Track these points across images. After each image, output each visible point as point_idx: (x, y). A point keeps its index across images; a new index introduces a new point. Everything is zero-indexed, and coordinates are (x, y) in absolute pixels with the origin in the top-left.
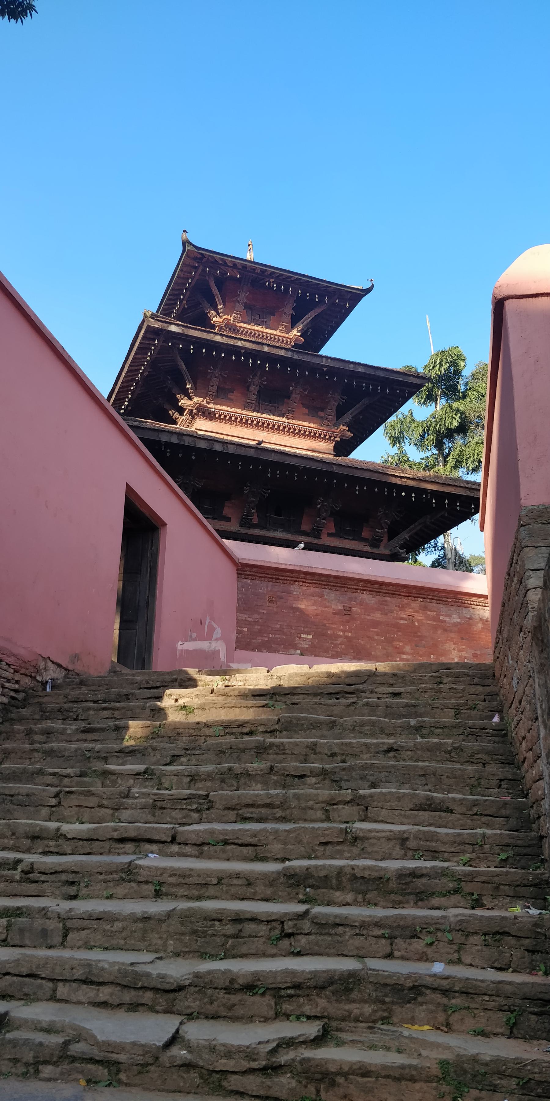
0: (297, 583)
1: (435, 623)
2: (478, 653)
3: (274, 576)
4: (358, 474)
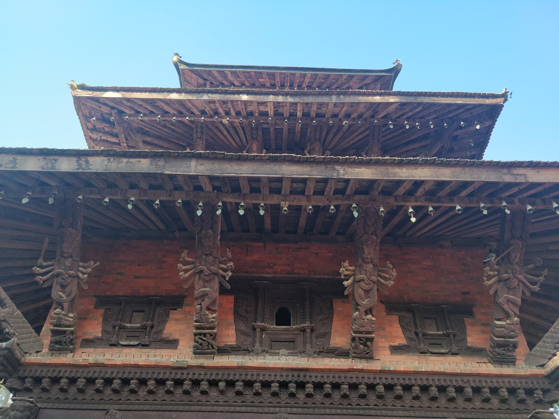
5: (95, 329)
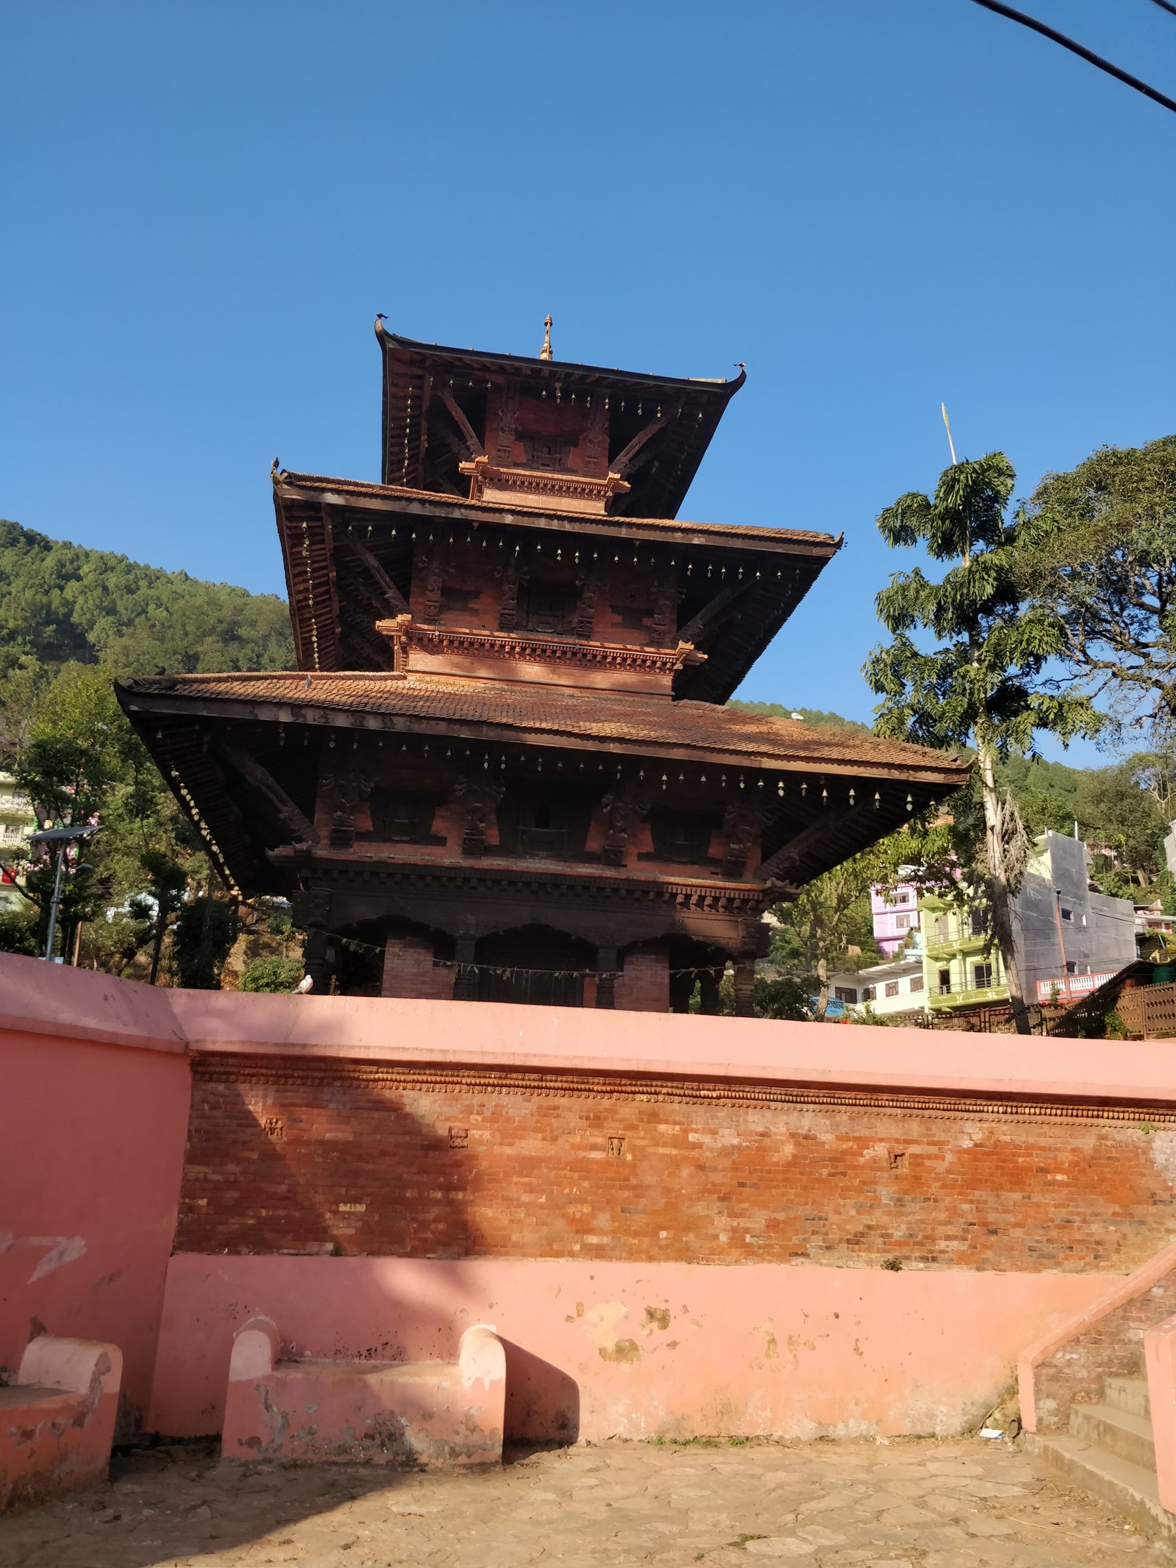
0: (338, 1083)
1: (674, 1152)
2: (781, 1216)
3: (280, 1072)
4: (663, 753)
5: (366, 824)
